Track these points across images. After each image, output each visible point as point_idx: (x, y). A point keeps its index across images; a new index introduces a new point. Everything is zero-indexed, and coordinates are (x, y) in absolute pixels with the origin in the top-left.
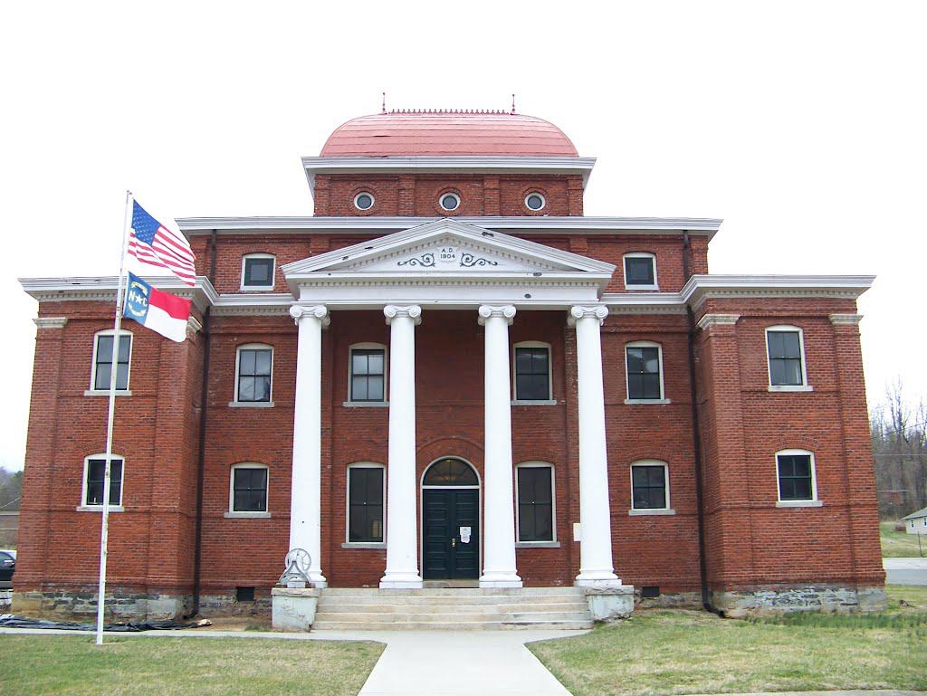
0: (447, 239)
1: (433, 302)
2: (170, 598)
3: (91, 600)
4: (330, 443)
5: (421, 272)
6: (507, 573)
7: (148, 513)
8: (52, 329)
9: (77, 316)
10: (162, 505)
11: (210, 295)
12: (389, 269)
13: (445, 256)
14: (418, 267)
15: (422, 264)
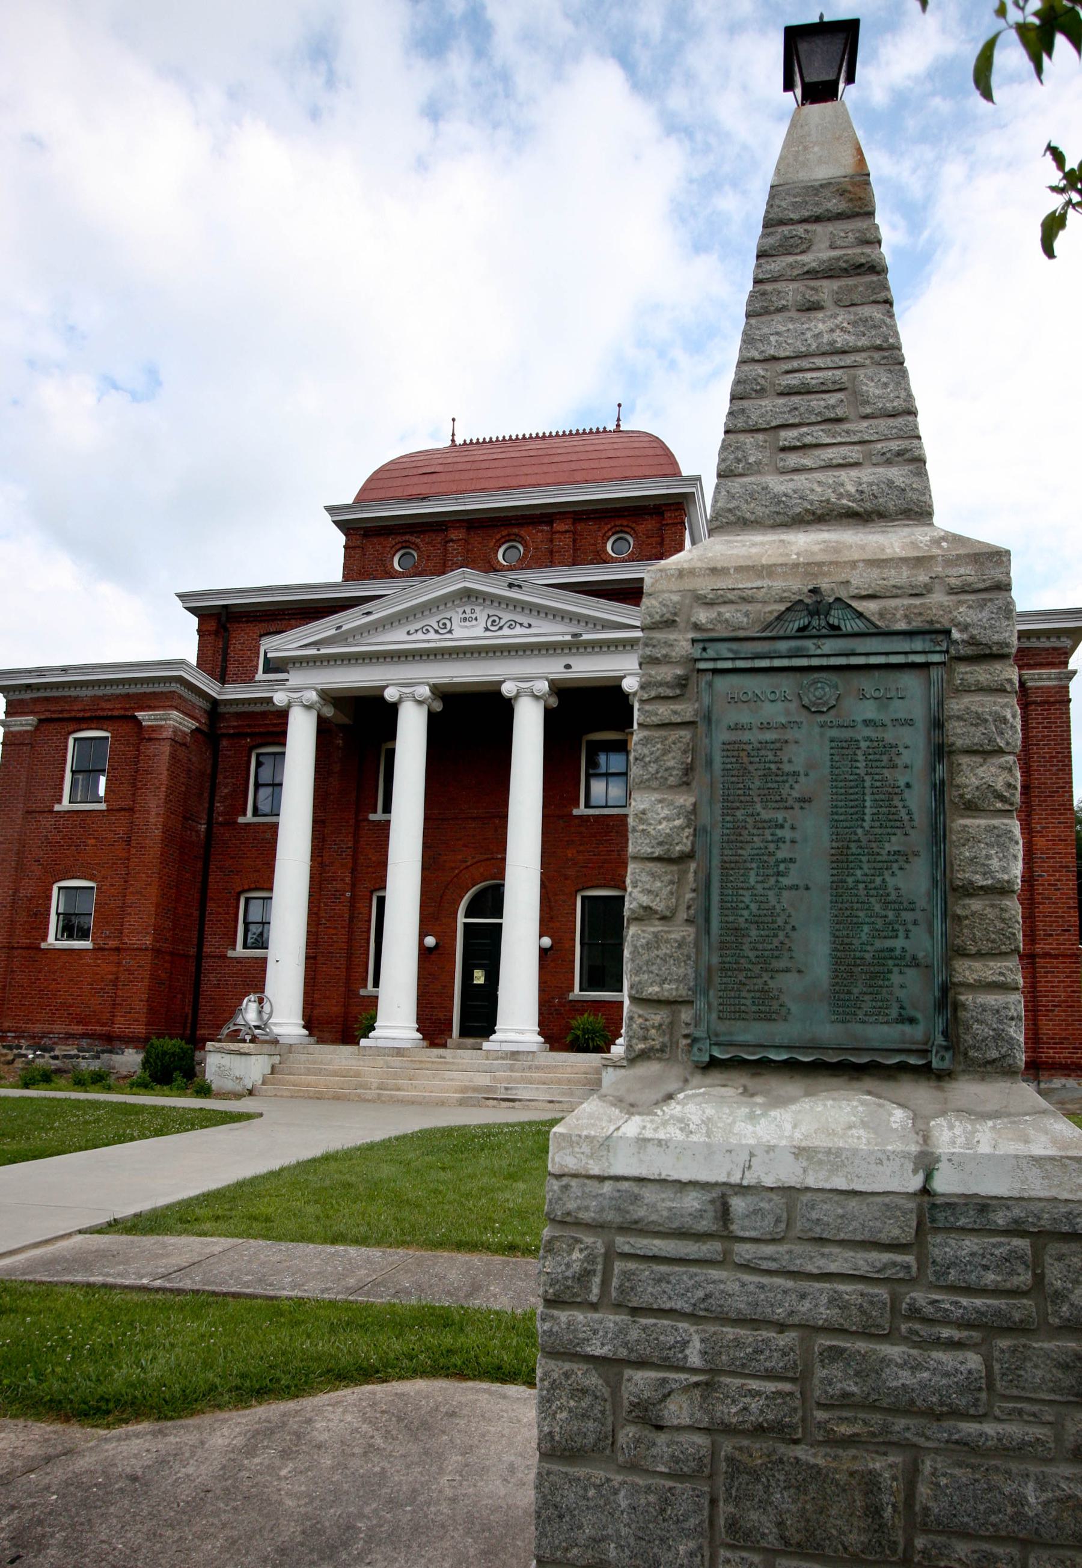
0: (468, 595)
1: (446, 680)
2: (137, 1053)
3: (52, 1054)
4: (350, 865)
5: (435, 641)
6: (521, 1032)
7: (118, 949)
8: (19, 732)
9: (48, 715)
10: (133, 941)
11: (207, 685)
12: (397, 639)
13: (465, 619)
14: (432, 635)
15: (437, 632)
